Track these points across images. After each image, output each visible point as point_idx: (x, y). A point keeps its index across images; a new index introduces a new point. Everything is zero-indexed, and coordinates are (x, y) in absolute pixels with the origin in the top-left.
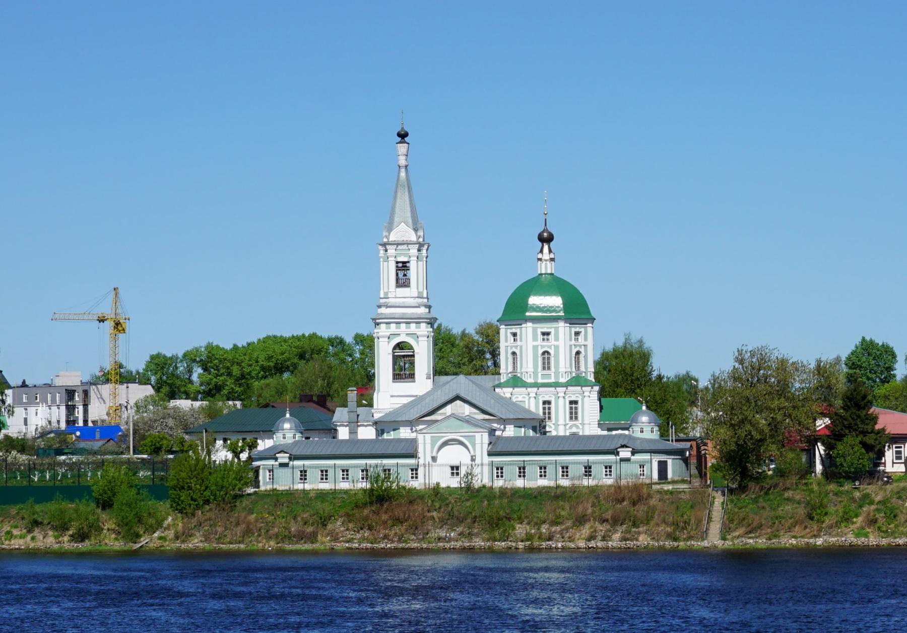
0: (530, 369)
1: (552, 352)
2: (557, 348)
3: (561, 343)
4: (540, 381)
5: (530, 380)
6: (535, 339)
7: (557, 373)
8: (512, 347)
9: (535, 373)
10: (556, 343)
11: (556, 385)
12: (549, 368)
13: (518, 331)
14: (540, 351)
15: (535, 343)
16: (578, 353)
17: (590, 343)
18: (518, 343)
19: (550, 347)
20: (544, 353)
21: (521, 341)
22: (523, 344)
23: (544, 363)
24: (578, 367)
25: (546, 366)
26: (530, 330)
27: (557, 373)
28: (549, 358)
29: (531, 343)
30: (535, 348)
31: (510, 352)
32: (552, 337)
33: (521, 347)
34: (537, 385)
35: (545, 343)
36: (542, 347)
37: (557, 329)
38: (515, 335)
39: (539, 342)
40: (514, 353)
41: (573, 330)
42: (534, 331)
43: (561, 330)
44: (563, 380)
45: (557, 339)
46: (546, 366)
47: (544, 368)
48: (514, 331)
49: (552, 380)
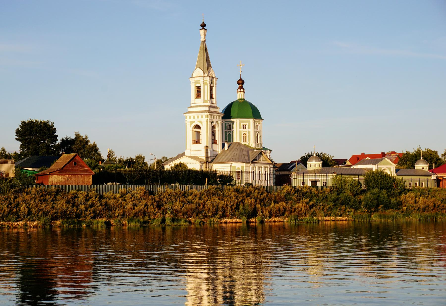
1: (247, 134)
2: (249, 132)
8: (228, 132)
14: (242, 134)
20: (244, 134)
23: (243, 139)
24: (257, 142)
28: (246, 137)
30: (240, 132)
32: (247, 127)
35: (244, 130)
36: (243, 132)
37: (249, 124)
39: (242, 129)
42: (240, 124)
45: (249, 128)
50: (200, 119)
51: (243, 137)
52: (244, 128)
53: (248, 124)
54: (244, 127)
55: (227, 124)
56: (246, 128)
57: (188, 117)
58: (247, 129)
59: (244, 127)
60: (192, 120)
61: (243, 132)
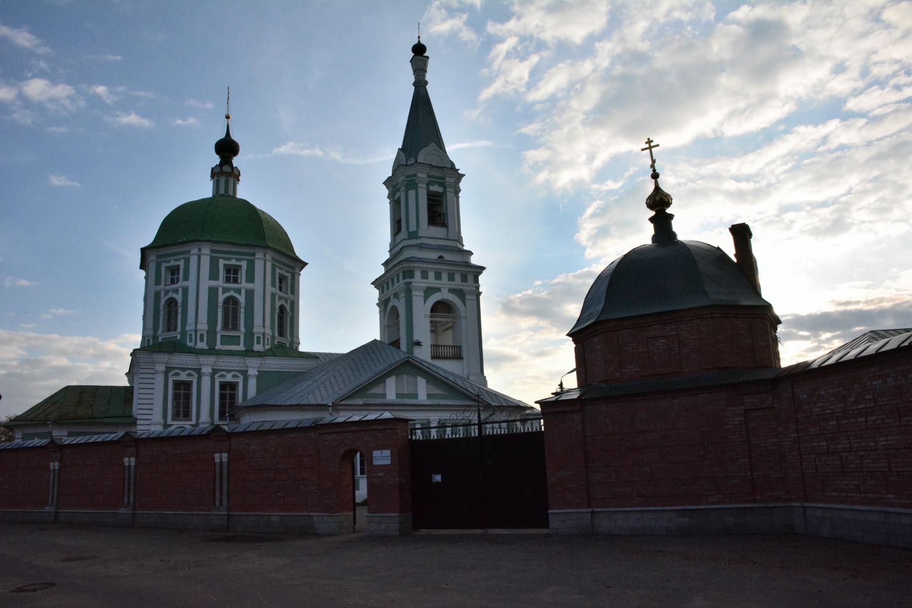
0: (203, 326)
1: (242, 299)
2: (250, 294)
3: (257, 286)
4: (219, 346)
5: (202, 345)
6: (214, 275)
7: (250, 334)
8: (167, 292)
9: (212, 332)
10: (250, 286)
11: (249, 352)
12: (235, 327)
13: (181, 263)
14: (221, 298)
15: (214, 283)
16: (282, 308)
18: (182, 283)
19: (238, 291)
20: (227, 301)
21: (186, 278)
22: (191, 284)
24: (281, 334)
25: (231, 321)
26: (206, 262)
27: (250, 334)
29: (206, 283)
30: (213, 292)
31: (163, 300)
33: (185, 291)
34: (211, 351)
36: (225, 290)
38: (174, 270)
39: (221, 283)
40: (172, 302)
43: (259, 265)
44: (258, 347)
45: (251, 278)
46: (231, 321)
47: (225, 326)
48: (173, 263)
49: (241, 347)
52: (228, 280)
53: (244, 264)
54: (232, 273)
55: (164, 265)
56: (236, 281)
58: (244, 285)
59: (232, 273)
61: (225, 290)
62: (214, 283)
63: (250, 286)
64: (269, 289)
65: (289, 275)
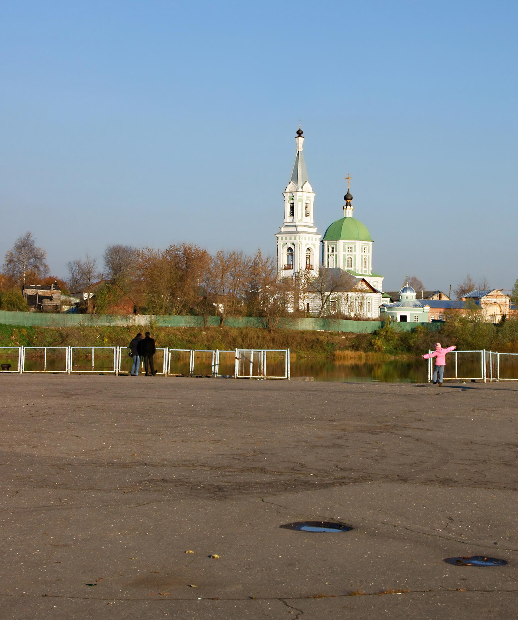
2: (355, 256)
3: (357, 253)
6: (344, 251)
10: (355, 253)
14: (347, 257)
15: (344, 253)
17: (370, 254)
18: (335, 253)
23: (348, 263)
30: (344, 255)
35: (350, 253)
36: (348, 255)
37: (355, 246)
39: (347, 253)
41: (364, 247)
42: (344, 246)
45: (355, 251)
47: (348, 266)
48: (332, 246)
50: (293, 241)
51: (348, 261)
57: (280, 238)
59: (350, 249)
60: (284, 241)
62: (344, 253)
63: (355, 253)
64: (361, 254)
65: (368, 247)
